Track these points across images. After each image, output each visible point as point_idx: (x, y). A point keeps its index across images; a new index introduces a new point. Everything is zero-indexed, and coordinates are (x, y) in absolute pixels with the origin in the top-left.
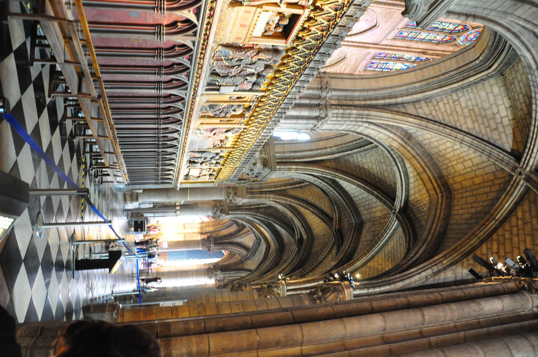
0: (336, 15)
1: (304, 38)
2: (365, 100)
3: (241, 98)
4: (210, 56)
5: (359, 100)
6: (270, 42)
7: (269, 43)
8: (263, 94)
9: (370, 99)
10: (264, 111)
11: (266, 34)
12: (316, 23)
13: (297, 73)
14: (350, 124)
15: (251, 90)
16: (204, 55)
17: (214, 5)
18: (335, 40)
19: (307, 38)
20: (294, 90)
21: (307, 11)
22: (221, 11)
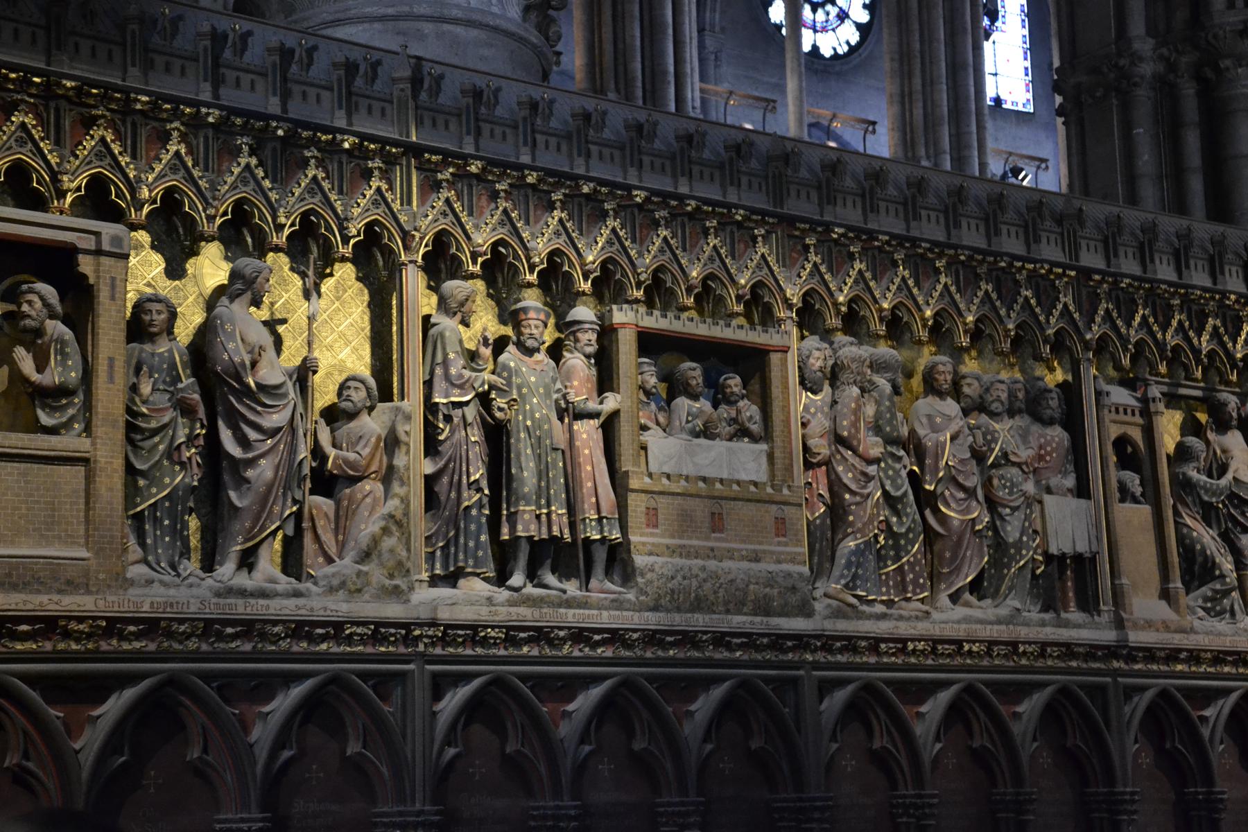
4: (883, 616)
17: (635, 636)
22: (655, 609)
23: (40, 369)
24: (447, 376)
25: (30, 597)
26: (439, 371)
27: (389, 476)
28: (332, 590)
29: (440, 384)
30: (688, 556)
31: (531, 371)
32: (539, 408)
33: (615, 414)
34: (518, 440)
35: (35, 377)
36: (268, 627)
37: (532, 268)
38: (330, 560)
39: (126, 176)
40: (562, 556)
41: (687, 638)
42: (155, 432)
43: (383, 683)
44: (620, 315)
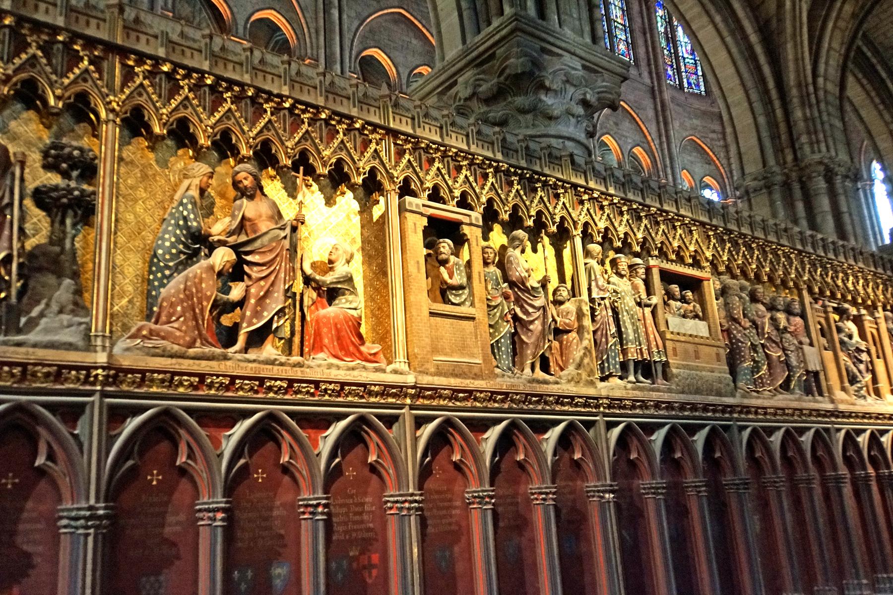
0: (646, 216)
1: (693, 254)
2: (771, 102)
3: (822, 330)
4: (758, 398)
5: (774, 111)
6: (712, 305)
7: (714, 305)
8: (805, 293)
9: (766, 91)
10: (839, 283)
11: (701, 314)
12: (667, 242)
13: (754, 245)
14: (827, 111)
15: (803, 316)
16: (759, 408)
17: (676, 405)
18: (683, 201)
19: (692, 248)
20: (784, 241)
21: (652, 262)
22: (683, 392)
23: (451, 278)
24: (597, 286)
25: (463, 381)
26: (593, 284)
27: (580, 330)
28: (569, 381)
29: (595, 291)
30: (690, 370)
31: (623, 285)
32: (630, 302)
33: (656, 306)
34: (623, 316)
35: (449, 281)
36: (548, 398)
37: (619, 239)
38: (562, 369)
39: (475, 191)
40: (645, 368)
41: (694, 407)
42: (495, 307)
43: (589, 425)
44: (652, 262)
